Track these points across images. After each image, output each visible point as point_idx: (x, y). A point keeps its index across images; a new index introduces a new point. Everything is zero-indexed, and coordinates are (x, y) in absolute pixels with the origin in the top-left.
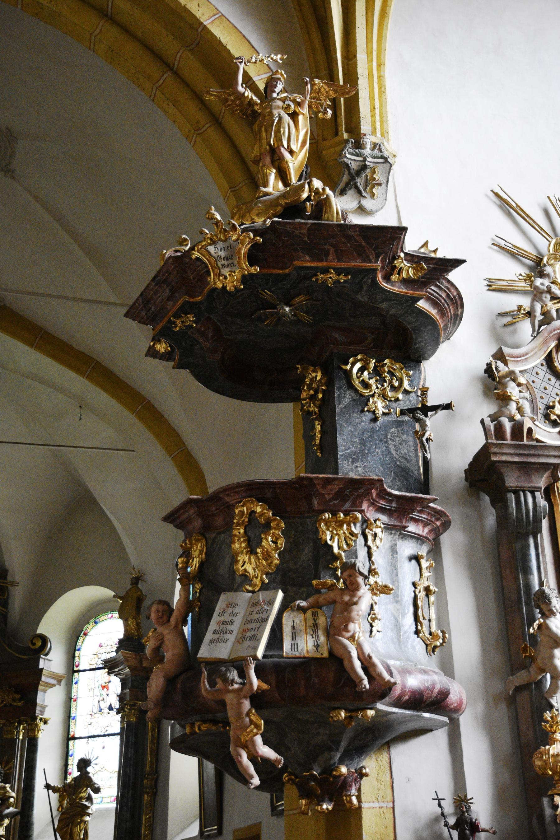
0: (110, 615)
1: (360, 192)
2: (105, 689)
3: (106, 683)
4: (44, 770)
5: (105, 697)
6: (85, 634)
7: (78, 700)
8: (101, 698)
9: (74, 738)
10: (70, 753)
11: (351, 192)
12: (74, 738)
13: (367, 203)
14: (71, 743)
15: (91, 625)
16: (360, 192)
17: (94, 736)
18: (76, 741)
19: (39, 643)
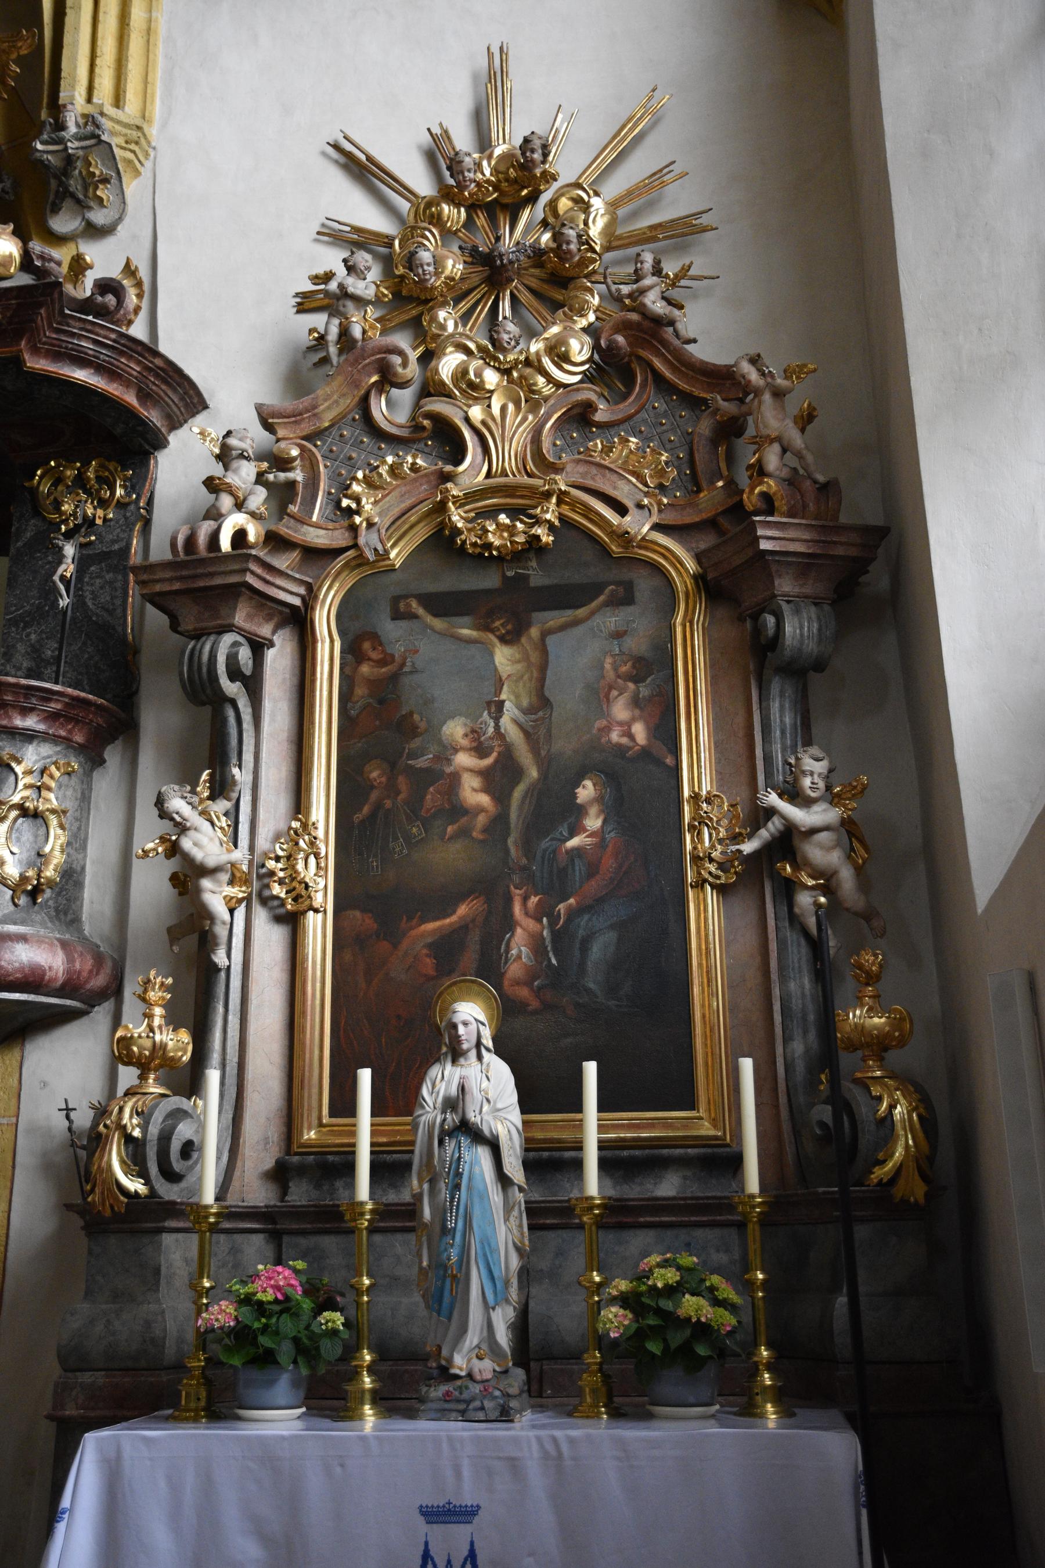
1: (78, 201)
11: (68, 203)
13: (99, 217)
16: (78, 201)
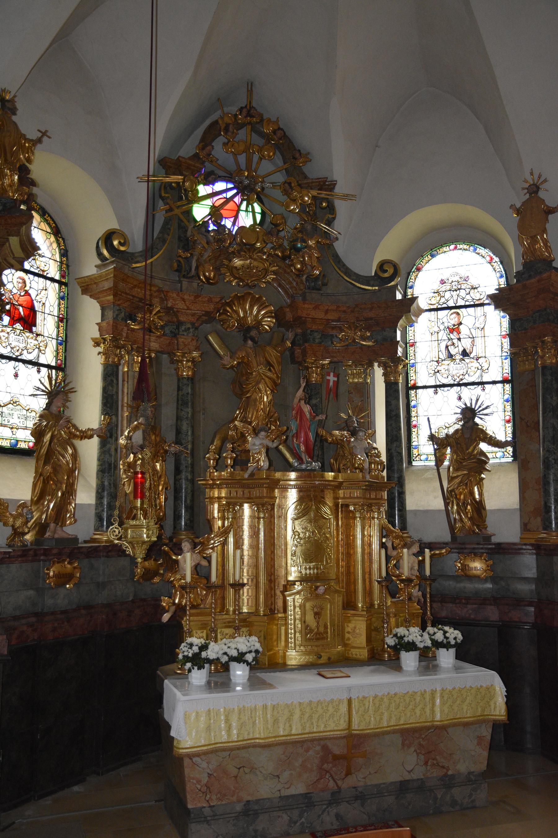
0: (452, 247)
2: (455, 333)
3: (454, 325)
4: (428, 419)
5: (455, 341)
6: (419, 270)
7: (417, 344)
8: (450, 343)
9: (415, 387)
10: (413, 403)
12: (415, 387)
14: (412, 392)
15: (426, 259)
17: (444, 386)
18: (420, 391)
19: (391, 271)
